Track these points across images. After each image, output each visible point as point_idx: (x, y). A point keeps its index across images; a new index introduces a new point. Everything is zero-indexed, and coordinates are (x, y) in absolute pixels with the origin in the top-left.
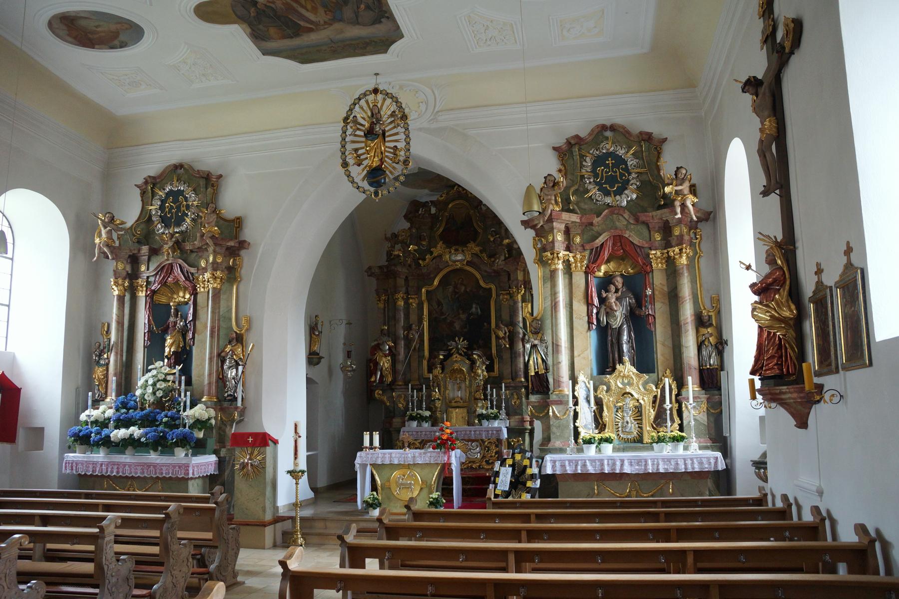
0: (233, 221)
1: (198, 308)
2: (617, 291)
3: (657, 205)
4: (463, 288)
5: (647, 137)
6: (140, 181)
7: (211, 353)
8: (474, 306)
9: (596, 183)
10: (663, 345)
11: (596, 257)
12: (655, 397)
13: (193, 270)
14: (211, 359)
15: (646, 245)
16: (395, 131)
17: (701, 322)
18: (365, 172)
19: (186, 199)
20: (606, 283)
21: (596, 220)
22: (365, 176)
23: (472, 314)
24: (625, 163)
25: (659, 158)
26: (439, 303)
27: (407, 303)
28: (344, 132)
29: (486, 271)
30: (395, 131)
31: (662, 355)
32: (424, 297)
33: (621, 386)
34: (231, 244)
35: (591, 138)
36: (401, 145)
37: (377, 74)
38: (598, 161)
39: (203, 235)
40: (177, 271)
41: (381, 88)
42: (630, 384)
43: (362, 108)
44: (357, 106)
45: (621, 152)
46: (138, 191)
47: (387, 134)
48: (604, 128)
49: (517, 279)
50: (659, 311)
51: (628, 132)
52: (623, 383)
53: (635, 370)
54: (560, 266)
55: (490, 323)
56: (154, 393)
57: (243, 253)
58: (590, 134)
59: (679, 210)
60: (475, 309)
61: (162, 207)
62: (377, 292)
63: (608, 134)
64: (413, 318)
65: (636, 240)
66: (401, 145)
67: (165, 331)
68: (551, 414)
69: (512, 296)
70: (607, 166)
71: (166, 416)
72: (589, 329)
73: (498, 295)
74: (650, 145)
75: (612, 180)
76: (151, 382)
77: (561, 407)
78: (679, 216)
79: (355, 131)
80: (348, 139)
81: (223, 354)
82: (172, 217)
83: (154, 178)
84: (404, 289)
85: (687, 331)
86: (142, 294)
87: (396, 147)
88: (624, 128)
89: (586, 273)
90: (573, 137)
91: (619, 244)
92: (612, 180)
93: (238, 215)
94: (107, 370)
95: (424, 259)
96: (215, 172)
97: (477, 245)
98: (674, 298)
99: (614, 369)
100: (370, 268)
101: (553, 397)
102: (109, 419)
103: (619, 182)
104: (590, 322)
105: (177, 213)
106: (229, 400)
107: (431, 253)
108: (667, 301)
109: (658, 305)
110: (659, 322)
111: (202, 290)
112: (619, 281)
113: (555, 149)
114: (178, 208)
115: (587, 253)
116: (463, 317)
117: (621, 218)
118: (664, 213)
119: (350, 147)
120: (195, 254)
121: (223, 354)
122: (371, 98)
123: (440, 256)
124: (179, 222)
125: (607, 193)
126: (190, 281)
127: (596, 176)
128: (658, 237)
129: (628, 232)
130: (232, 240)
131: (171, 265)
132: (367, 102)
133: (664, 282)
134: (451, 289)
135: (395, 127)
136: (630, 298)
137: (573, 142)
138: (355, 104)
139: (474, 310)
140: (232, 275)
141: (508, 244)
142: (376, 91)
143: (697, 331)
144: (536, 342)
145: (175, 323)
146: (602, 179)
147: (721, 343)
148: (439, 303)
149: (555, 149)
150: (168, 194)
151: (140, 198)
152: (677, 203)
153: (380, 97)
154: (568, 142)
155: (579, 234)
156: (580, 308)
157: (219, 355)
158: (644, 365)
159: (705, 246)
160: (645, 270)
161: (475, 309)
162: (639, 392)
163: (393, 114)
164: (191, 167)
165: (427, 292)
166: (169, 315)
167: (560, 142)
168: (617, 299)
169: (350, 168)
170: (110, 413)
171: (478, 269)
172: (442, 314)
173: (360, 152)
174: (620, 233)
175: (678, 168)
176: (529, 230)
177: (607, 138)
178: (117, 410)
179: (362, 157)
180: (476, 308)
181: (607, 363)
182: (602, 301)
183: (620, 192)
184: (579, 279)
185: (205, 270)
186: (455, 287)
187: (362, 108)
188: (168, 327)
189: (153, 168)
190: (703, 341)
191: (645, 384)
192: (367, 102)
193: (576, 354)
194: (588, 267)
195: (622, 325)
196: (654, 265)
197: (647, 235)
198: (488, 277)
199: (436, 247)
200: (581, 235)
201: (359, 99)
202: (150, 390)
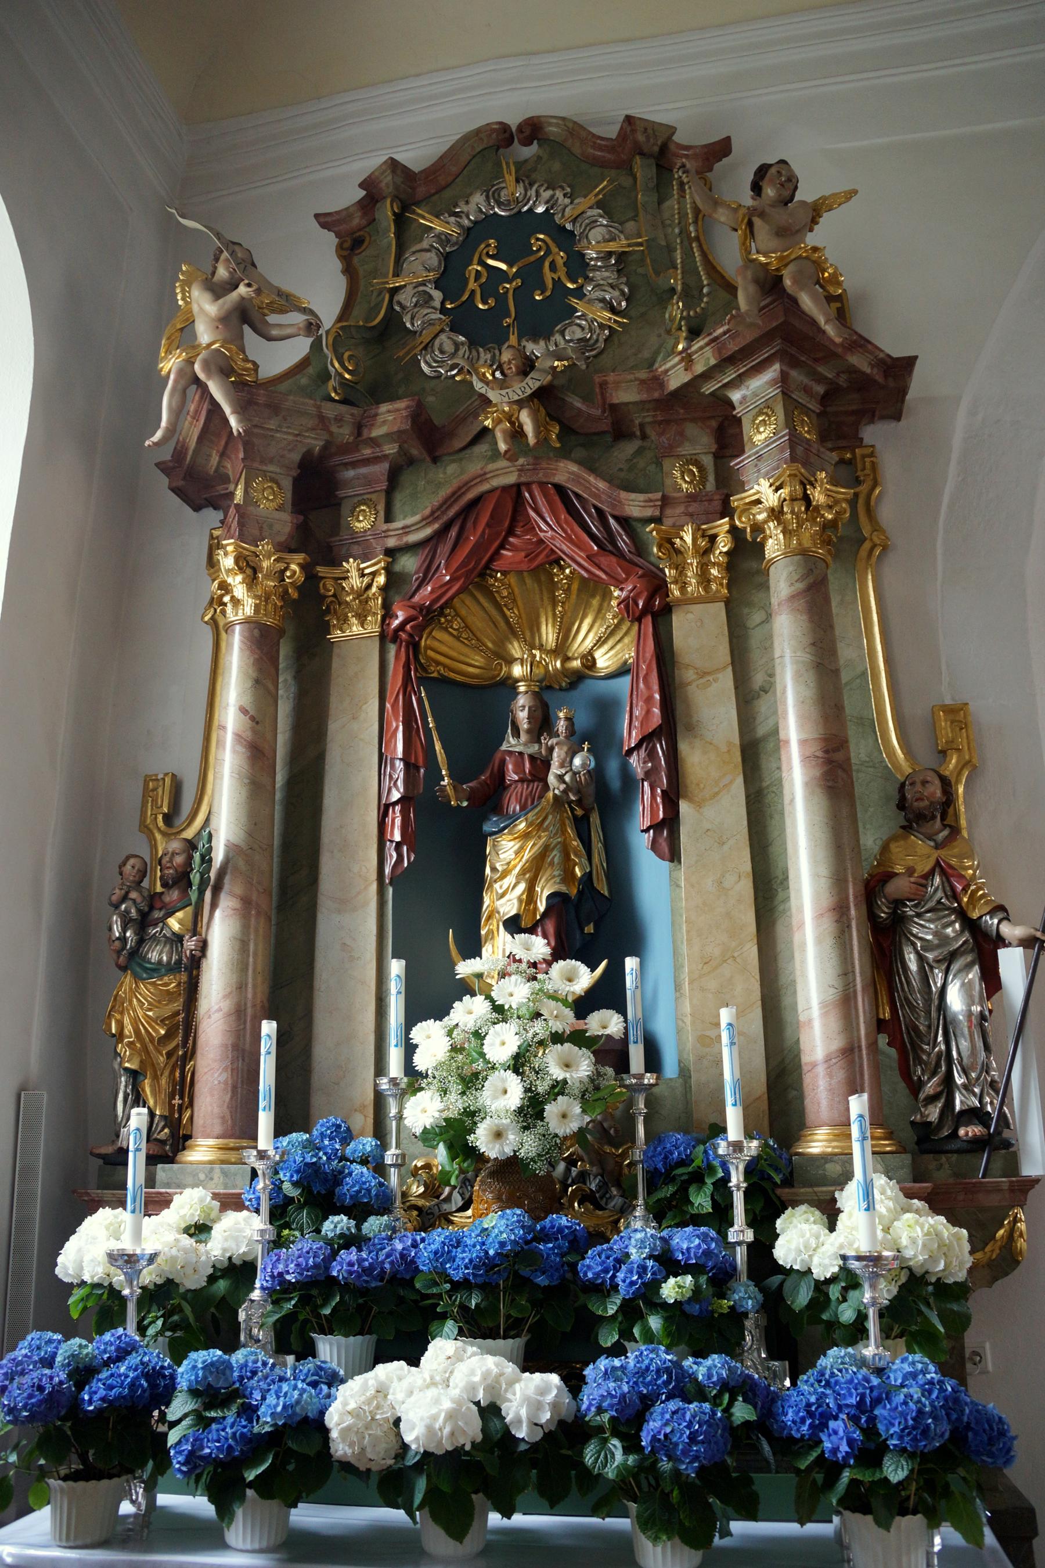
56: (532, 1111)
67: (490, 801)
71: (669, 1263)
76: (503, 1041)
82: (500, 308)
86: (357, 633)
102: (239, 1272)
105: (523, 294)
114: (531, 276)
131: (515, 491)
145: (541, 765)
151: (337, 265)
166: (501, 722)
170: (241, 1232)
178: (280, 1213)
188: (499, 783)
189: (419, 126)
202: (504, 1095)
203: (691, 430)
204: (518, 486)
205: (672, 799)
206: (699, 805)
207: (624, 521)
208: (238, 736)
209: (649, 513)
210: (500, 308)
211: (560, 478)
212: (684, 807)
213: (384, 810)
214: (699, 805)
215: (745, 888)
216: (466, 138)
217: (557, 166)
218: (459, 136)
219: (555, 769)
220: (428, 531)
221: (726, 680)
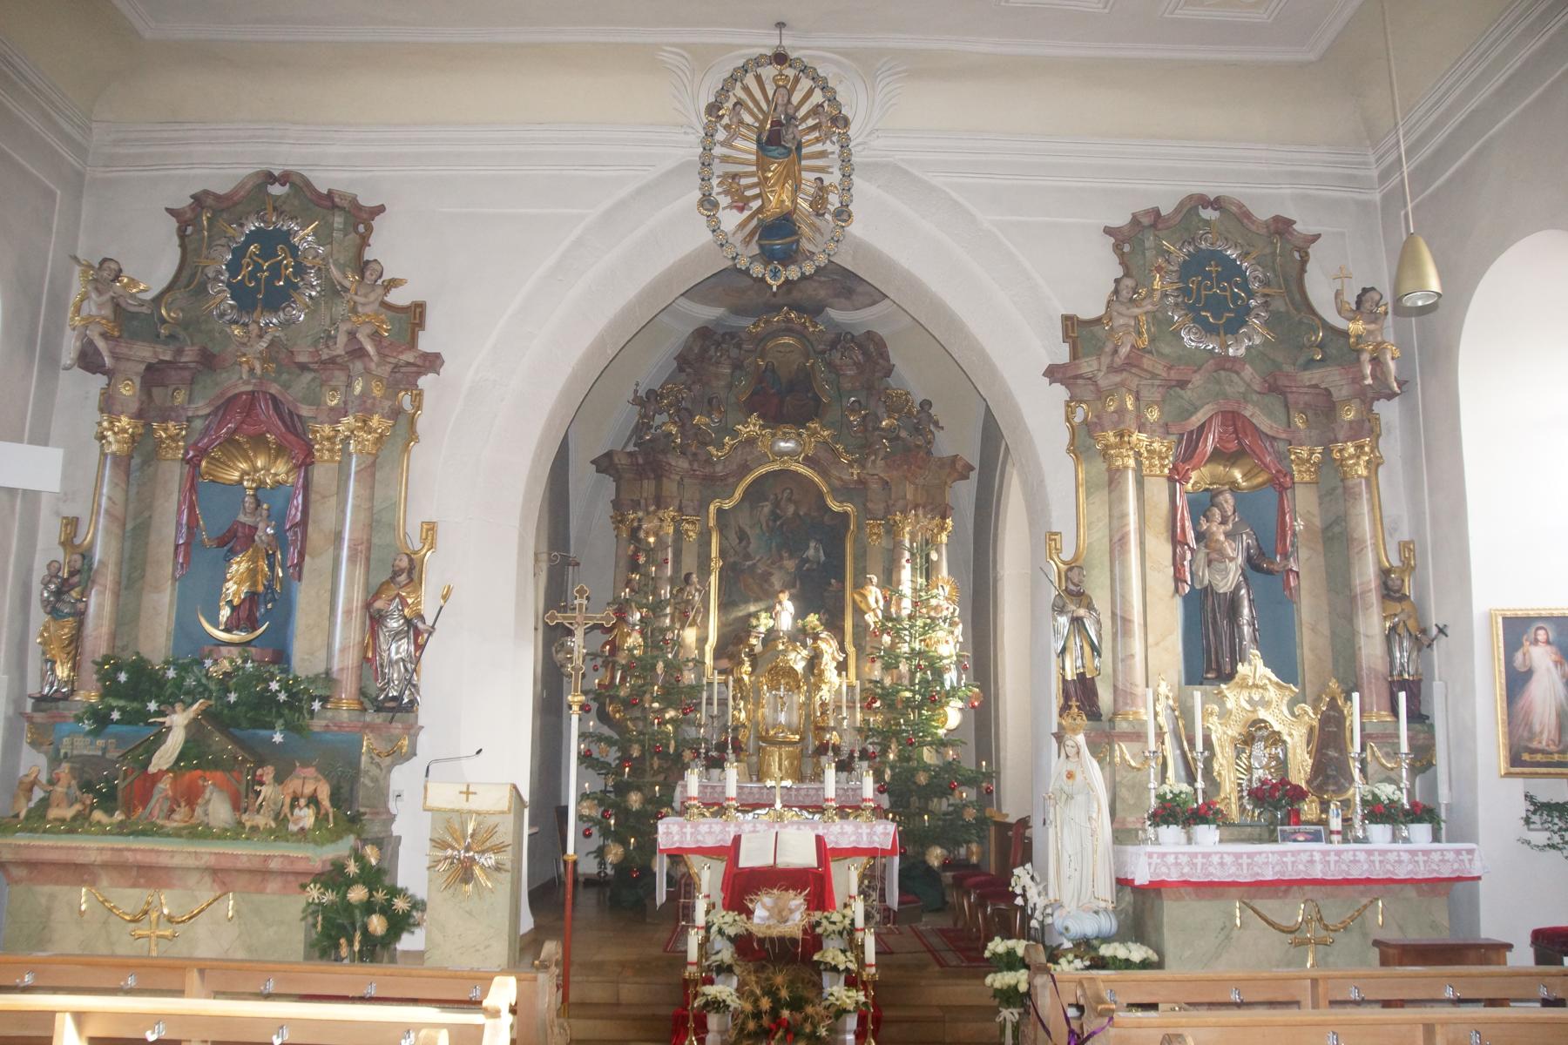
0: (408, 308)
1: (313, 497)
2: (1224, 522)
3: (1301, 360)
4: (791, 509)
5: (1281, 226)
6: (183, 202)
7: (349, 600)
8: (812, 544)
9: (1191, 308)
10: (1314, 630)
11: (1188, 451)
12: (1311, 729)
13: (305, 411)
14: (348, 612)
15: (1284, 436)
16: (818, 147)
17: (1390, 592)
18: (755, 222)
19: (293, 250)
20: (1203, 505)
21: (1197, 379)
22: (752, 234)
23: (807, 560)
24: (1242, 273)
25: (1303, 270)
26: (742, 536)
27: (677, 531)
28: (709, 135)
29: (841, 479)
30: (818, 147)
31: (1312, 650)
32: (711, 523)
33: (1248, 707)
34: (408, 357)
35: (1179, 218)
36: (833, 178)
37: (781, 25)
38: (1194, 266)
39: (352, 335)
40: (264, 409)
41: (793, 55)
42: (1266, 704)
43: (746, 89)
44: (739, 84)
45: (1232, 253)
46: (173, 223)
47: (804, 151)
48: (1203, 201)
49: (904, 497)
50: (1305, 564)
51: (1248, 215)
52: (1250, 701)
53: (1274, 678)
54: (1131, 462)
55: (842, 580)
57: (424, 382)
58: (1177, 210)
59: (1368, 370)
60: (813, 551)
61: (234, 267)
62: (617, 504)
63: (1208, 214)
64: (689, 563)
65: (1264, 423)
66: (833, 178)
68: (1118, 760)
69: (892, 531)
70: (1208, 276)
72: (1177, 590)
73: (860, 527)
74: (1285, 246)
75: (1217, 305)
77: (1137, 746)
78: (1369, 381)
79: (733, 136)
80: (718, 151)
81: (379, 604)
82: (257, 290)
83: (217, 197)
84: (677, 503)
85: (1367, 608)
87: (821, 180)
88: (1241, 206)
89: (1170, 479)
90: (1147, 212)
91: (1231, 429)
92: (1217, 305)
93: (419, 299)
94: (81, 625)
95: (721, 446)
96: (367, 201)
97: (824, 427)
98: (1337, 539)
99: (1233, 672)
100: (609, 455)
101: (1122, 726)
103: (1230, 310)
104: (1178, 579)
106: (391, 710)
107: (734, 434)
108: (1320, 547)
109: (1303, 553)
110: (1304, 584)
111: (327, 455)
112: (1228, 501)
113: (1108, 231)
114: (276, 271)
115: (1174, 438)
116: (790, 564)
117: (1235, 377)
118: (1334, 379)
119: (719, 168)
120: (308, 376)
121: (379, 604)
122: (769, 72)
123: (751, 441)
124: (277, 299)
125: (1209, 330)
126: (297, 435)
127: (1185, 292)
128: (1299, 422)
129: (1250, 407)
130: (401, 350)
132: (758, 78)
133: (1315, 509)
134: (767, 508)
135: (817, 140)
136: (1249, 536)
137: (1146, 221)
138: (733, 78)
139: (811, 552)
140: (404, 427)
141: (890, 429)
142: (780, 58)
143: (1384, 610)
144: (1082, 612)
146: (1198, 300)
147: (1424, 631)
148: (742, 536)
149: (1108, 231)
150: (253, 237)
151: (176, 240)
152: (1365, 357)
153: (791, 73)
154: (1135, 220)
155: (1156, 403)
156: (1161, 550)
157: (368, 606)
158: (1285, 667)
159: (1392, 446)
160: (1281, 484)
161: (813, 551)
162: (1282, 722)
163: (816, 110)
164: (308, 183)
165: (720, 511)
167: (1121, 220)
168: (1227, 535)
169: (721, 214)
171: (824, 473)
172: (747, 557)
173: (744, 181)
174: (1235, 407)
175: (1365, 291)
176: (1057, 386)
177: (1207, 222)
179: (749, 193)
180: (817, 549)
181: (1209, 660)
182: (1200, 537)
183: (1233, 327)
184: (1158, 490)
185: (336, 414)
186: (777, 504)
187: (746, 89)
190: (1393, 629)
191: (1292, 704)
192: (758, 78)
193: (1150, 640)
194: (1175, 469)
195: (1238, 588)
196: (1297, 478)
197: (1284, 419)
198: (843, 493)
199: (745, 423)
200: (1161, 404)
201: (745, 69)
203: (337, 373)
204: (253, 392)
205: (302, 556)
206: (313, 558)
207: (299, 417)
208: (107, 511)
209: (311, 414)
210: (257, 290)
211: (273, 391)
212: (307, 558)
213: (177, 546)
214: (313, 558)
215: (327, 595)
216: (250, 176)
217: (296, 203)
218: (251, 171)
219: (259, 533)
220: (207, 411)
221: (333, 501)
